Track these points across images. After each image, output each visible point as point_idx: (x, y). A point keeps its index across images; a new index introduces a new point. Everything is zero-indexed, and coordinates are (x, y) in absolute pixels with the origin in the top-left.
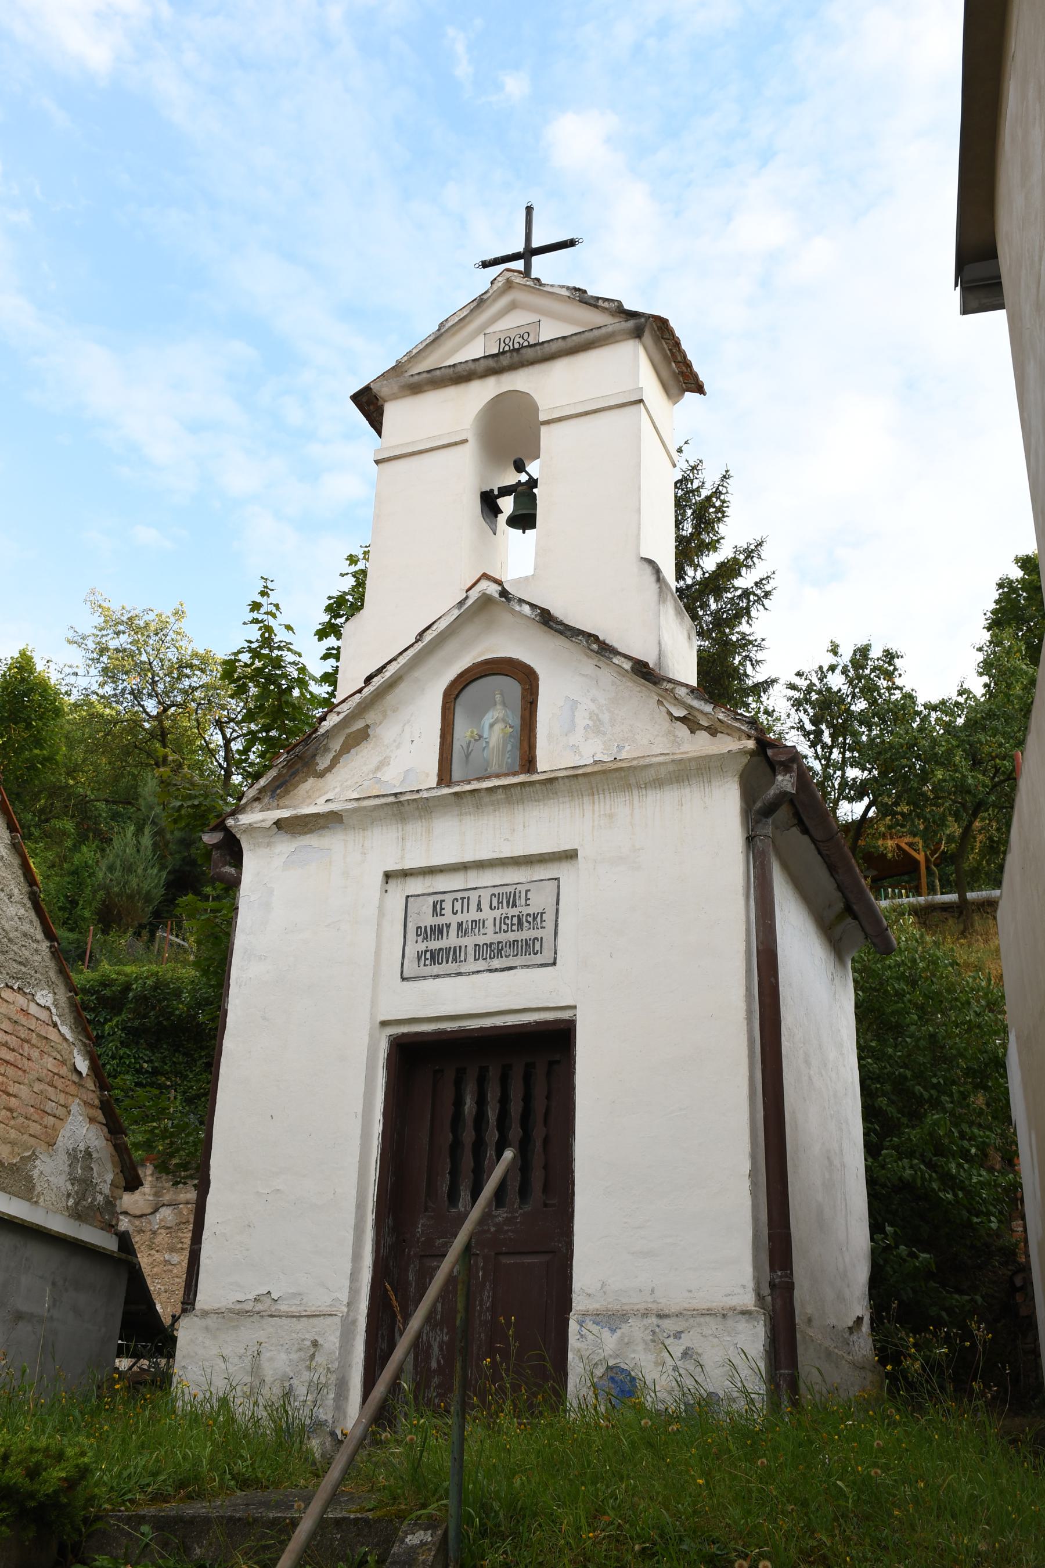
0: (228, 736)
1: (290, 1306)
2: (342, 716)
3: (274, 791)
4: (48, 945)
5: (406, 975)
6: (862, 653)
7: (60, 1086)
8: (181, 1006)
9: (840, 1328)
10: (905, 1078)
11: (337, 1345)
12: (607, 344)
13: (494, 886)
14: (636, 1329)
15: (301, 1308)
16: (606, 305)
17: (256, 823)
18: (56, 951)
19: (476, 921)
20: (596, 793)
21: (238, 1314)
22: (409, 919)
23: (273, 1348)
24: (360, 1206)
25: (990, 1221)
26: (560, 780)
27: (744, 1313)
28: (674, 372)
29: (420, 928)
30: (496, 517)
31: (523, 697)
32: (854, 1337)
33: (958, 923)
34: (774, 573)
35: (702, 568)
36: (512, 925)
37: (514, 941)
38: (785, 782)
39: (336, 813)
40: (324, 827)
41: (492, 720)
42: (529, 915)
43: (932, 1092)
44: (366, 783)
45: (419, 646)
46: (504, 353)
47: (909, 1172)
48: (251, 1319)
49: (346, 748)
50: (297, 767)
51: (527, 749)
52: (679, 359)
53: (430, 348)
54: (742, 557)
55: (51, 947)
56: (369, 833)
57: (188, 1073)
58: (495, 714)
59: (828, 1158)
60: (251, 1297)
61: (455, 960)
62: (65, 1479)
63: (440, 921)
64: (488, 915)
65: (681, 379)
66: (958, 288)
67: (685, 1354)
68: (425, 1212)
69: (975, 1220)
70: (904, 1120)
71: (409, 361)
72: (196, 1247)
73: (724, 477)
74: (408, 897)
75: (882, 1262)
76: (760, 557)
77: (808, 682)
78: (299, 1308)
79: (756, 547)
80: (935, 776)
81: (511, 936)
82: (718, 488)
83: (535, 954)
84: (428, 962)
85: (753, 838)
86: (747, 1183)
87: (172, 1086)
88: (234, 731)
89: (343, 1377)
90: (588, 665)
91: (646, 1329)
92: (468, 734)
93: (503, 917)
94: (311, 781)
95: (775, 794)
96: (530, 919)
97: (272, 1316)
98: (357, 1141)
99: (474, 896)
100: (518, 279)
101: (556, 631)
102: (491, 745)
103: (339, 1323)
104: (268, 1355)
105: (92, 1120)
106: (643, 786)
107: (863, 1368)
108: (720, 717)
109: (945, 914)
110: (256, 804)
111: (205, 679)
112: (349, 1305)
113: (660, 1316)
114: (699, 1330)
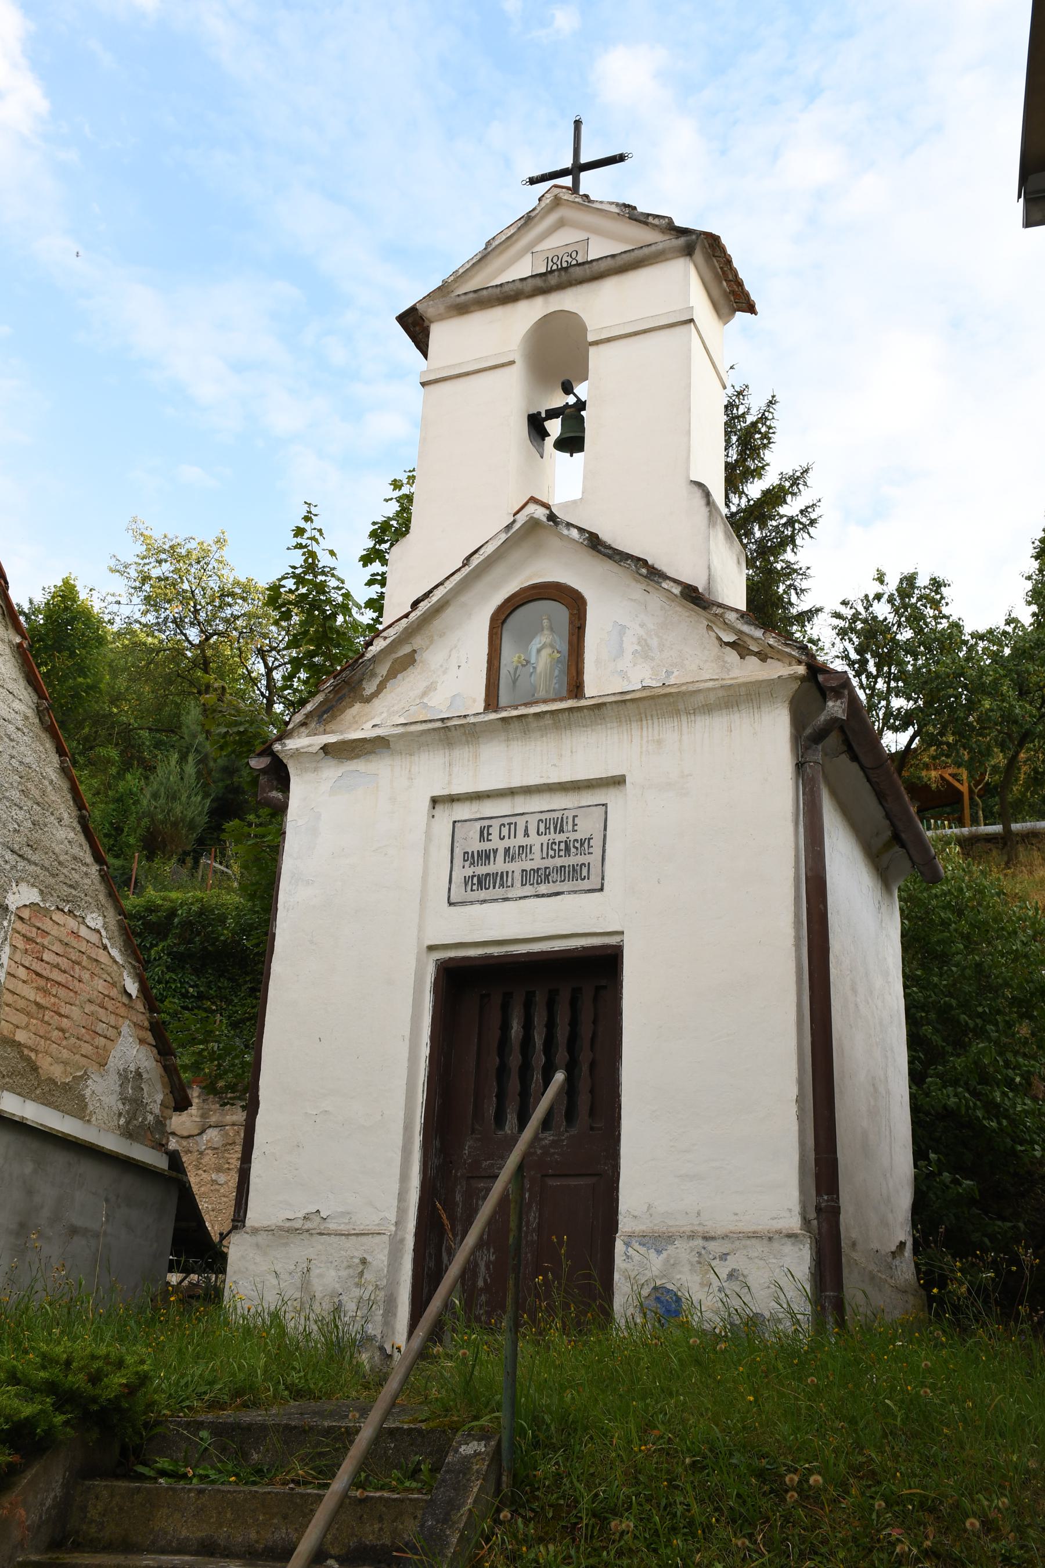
0: (270, 665)
1: (340, 1224)
2: (388, 641)
3: (320, 716)
4: (98, 868)
5: (453, 900)
6: (909, 581)
7: (111, 1008)
8: (225, 932)
9: (883, 1253)
10: (950, 1007)
11: (386, 1263)
12: (657, 263)
13: (541, 812)
14: (682, 1251)
15: (351, 1227)
16: (656, 222)
17: (303, 748)
18: (105, 874)
19: (523, 847)
20: (644, 719)
21: (288, 1231)
22: (456, 844)
23: (322, 1265)
24: (408, 1128)
25: (1034, 1150)
26: (608, 705)
27: (789, 1236)
28: (725, 291)
29: (468, 853)
30: (544, 440)
31: (571, 622)
32: (897, 1262)
33: (1002, 854)
34: (820, 501)
35: (747, 495)
36: (560, 850)
37: (561, 867)
38: (835, 708)
39: (383, 738)
40: (371, 752)
42: (576, 840)
43: (978, 1021)
45: (467, 570)
46: (552, 272)
47: (954, 1100)
48: (301, 1237)
49: (393, 674)
50: (343, 692)
51: (575, 674)
52: (730, 277)
53: (477, 267)
54: (787, 484)
55: (100, 871)
57: (233, 998)
59: (873, 1085)
60: (301, 1215)
61: (502, 885)
62: (126, 1385)
63: (486, 846)
64: (534, 840)
65: (732, 299)
66: (1022, 200)
67: (731, 1276)
68: (472, 1134)
69: (1019, 1148)
70: (949, 1049)
71: (455, 281)
72: (246, 1166)
73: (771, 402)
74: (455, 822)
75: (925, 1188)
76: (805, 484)
77: (854, 611)
78: (348, 1227)
79: (802, 474)
80: (983, 705)
81: (559, 862)
82: (763, 414)
83: (583, 879)
84: (475, 887)
85: (802, 765)
86: (793, 1109)
87: (217, 1010)
88: (276, 659)
89: (392, 1294)
90: (637, 590)
91: (692, 1251)
92: (516, 659)
93: (550, 842)
94: (357, 706)
95: (825, 720)
96: (578, 845)
98: (406, 1064)
99: (521, 822)
100: (567, 196)
102: (539, 670)
103: (387, 1242)
104: (318, 1271)
105: (142, 1041)
106: (692, 712)
107: (905, 1292)
108: (770, 643)
109: (990, 846)
110: (303, 729)
111: (247, 608)
112: (397, 1224)
113: (706, 1238)
114: (745, 1252)
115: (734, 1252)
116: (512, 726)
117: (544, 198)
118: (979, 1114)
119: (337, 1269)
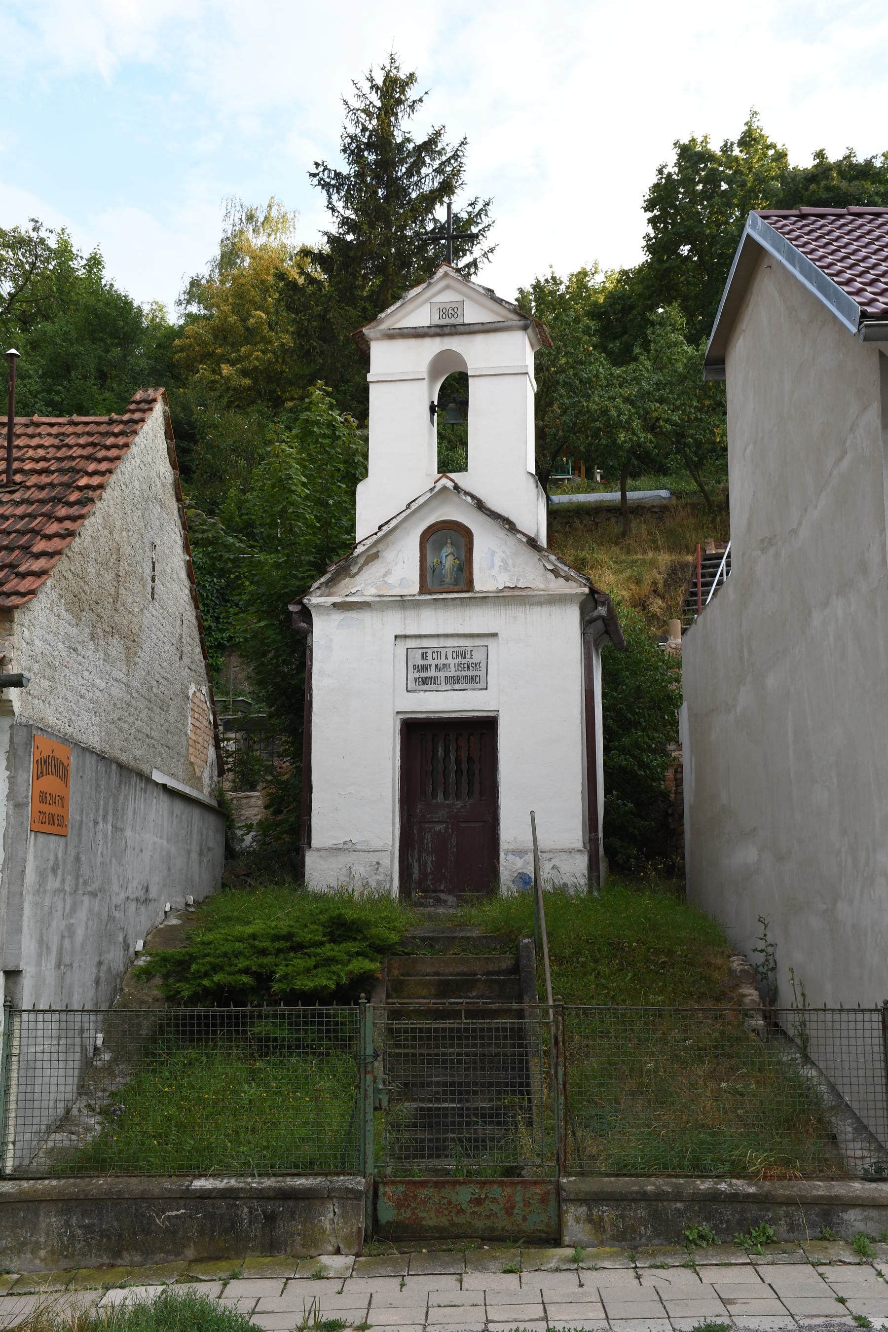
2: (366, 547)
16: (507, 305)
27: (578, 851)
38: (602, 610)
45: (409, 511)
49: (366, 563)
56: (385, 613)
58: (447, 550)
60: (342, 842)
61: (435, 683)
63: (425, 662)
64: (450, 661)
73: (462, 143)
76: (486, 215)
81: (464, 673)
90: (502, 534)
94: (347, 579)
99: (443, 651)
109: (609, 515)
115: (554, 858)
118: (636, 768)
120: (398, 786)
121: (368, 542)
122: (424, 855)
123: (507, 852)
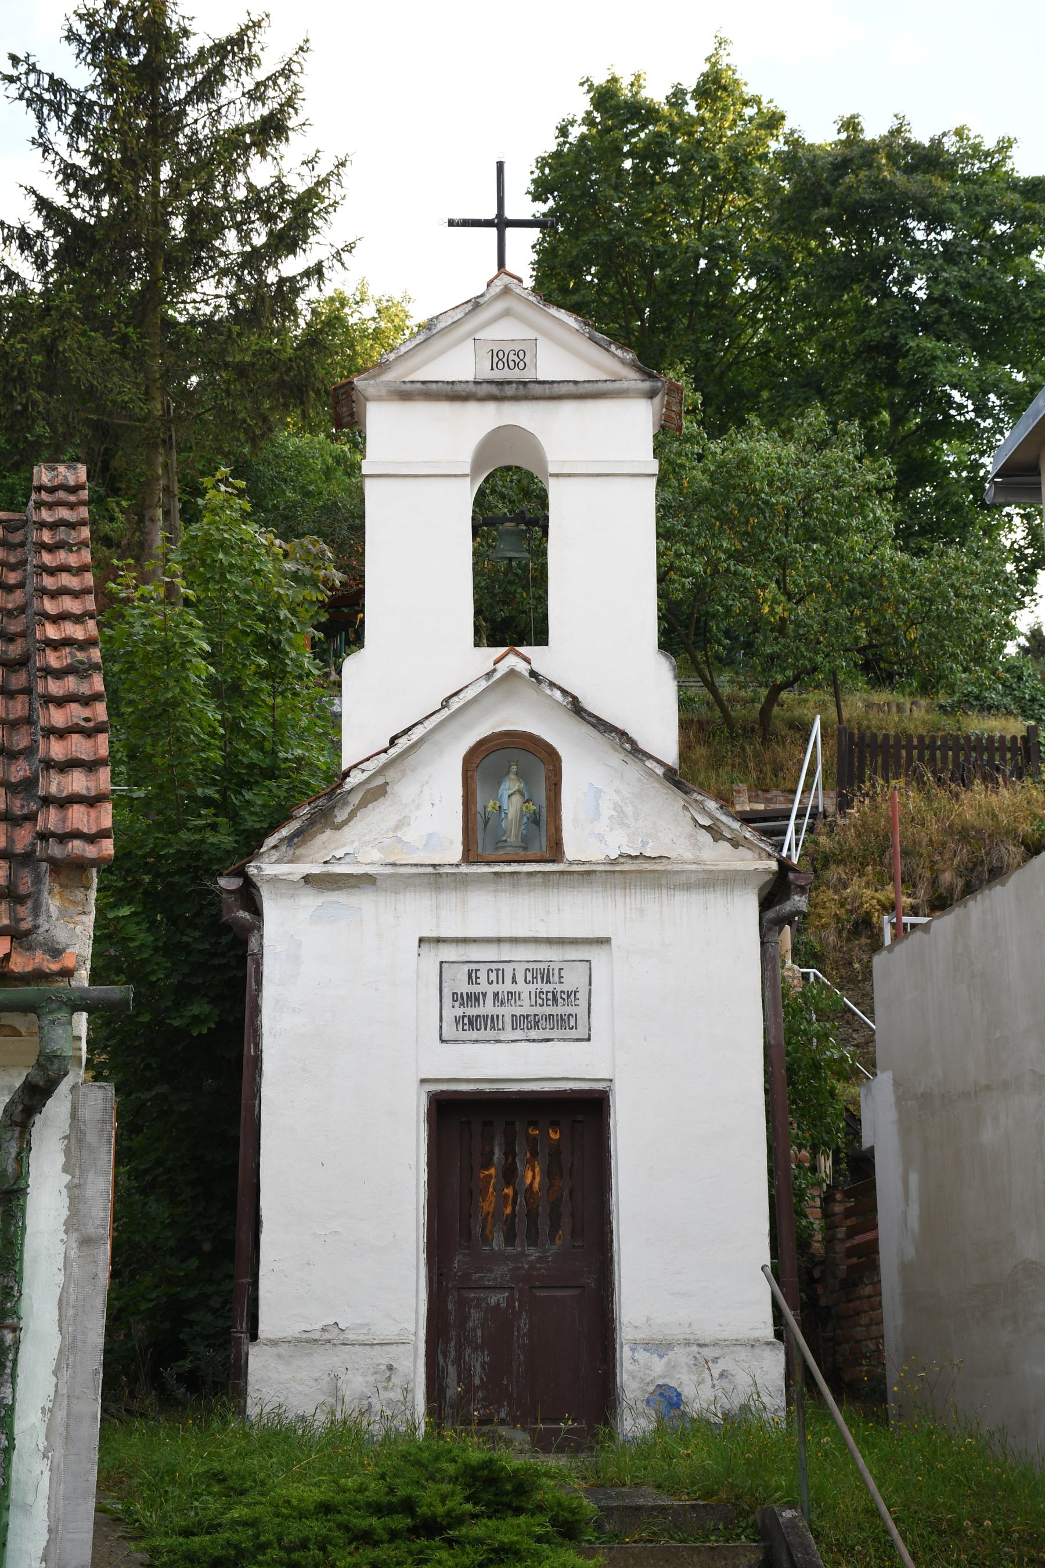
1: (359, 1335)
2: (367, 775)
5: (445, 1038)
14: (681, 1355)
22: (444, 984)
27: (768, 1343)
36: (547, 1000)
41: (511, 792)
42: (562, 992)
44: (386, 841)
48: (324, 1347)
49: (364, 803)
56: (401, 897)
58: (510, 785)
60: (318, 1326)
61: (493, 1027)
64: (521, 987)
67: (722, 1375)
73: (301, 49)
74: (442, 962)
76: (339, 183)
81: (547, 1010)
83: (571, 1029)
90: (615, 759)
94: (328, 832)
97: (344, 1344)
99: (508, 969)
101: (589, 723)
102: (510, 816)
110: (273, 852)
113: (699, 1345)
115: (724, 1356)
116: (503, 879)
117: (493, 284)
119: (364, 1375)
120: (423, 1219)
121: (372, 766)
122: (468, 1351)
123: (635, 1345)
